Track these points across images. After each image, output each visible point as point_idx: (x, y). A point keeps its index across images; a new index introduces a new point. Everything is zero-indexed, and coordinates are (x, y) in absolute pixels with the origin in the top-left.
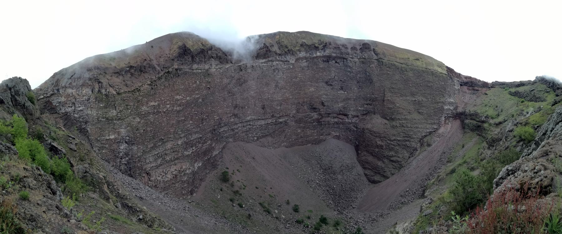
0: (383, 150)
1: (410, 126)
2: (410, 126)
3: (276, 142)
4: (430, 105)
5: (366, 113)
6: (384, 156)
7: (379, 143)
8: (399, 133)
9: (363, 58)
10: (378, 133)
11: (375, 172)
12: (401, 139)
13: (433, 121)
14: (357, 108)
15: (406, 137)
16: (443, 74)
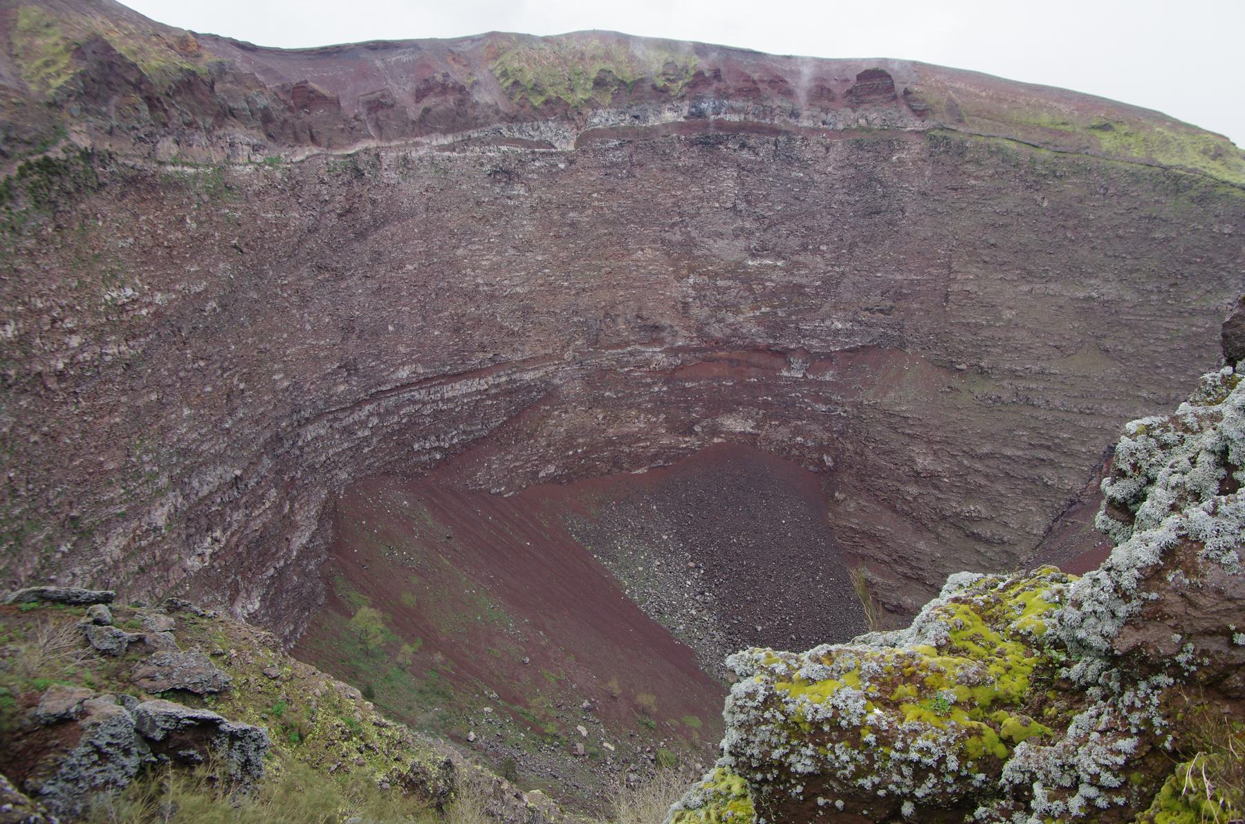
0: (941, 491)
1: (1063, 405)
2: (1063, 405)
3: (517, 464)
4: (1154, 323)
5: (864, 343)
6: (944, 518)
7: (926, 463)
8: (1010, 431)
9: (862, 129)
10: (922, 425)
11: (906, 577)
12: (1020, 453)
13: (1163, 393)
14: (828, 323)
15: (1041, 445)
16: (1233, 186)
